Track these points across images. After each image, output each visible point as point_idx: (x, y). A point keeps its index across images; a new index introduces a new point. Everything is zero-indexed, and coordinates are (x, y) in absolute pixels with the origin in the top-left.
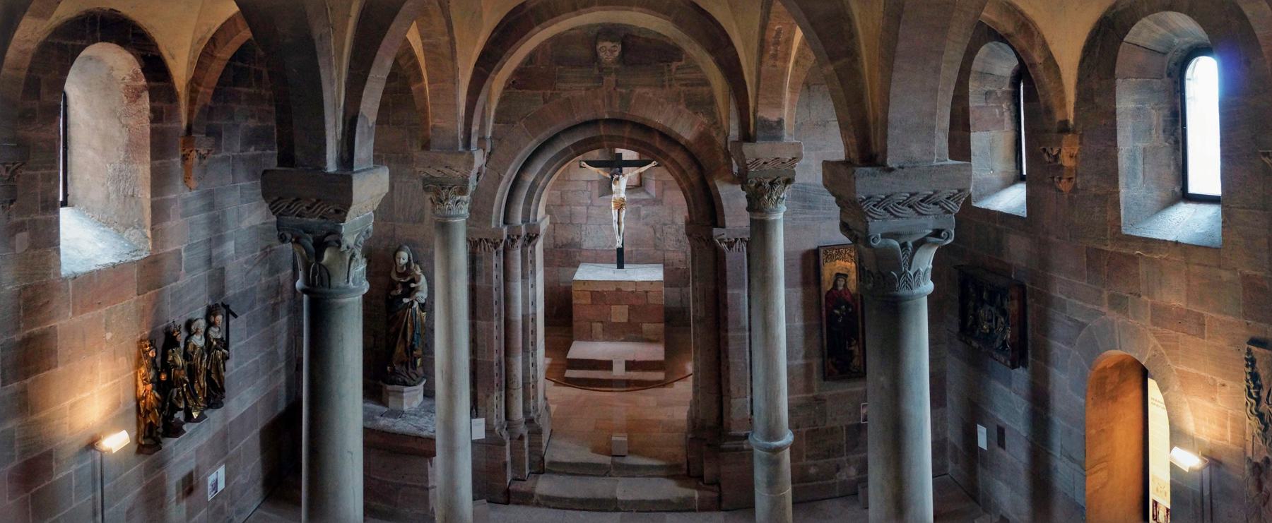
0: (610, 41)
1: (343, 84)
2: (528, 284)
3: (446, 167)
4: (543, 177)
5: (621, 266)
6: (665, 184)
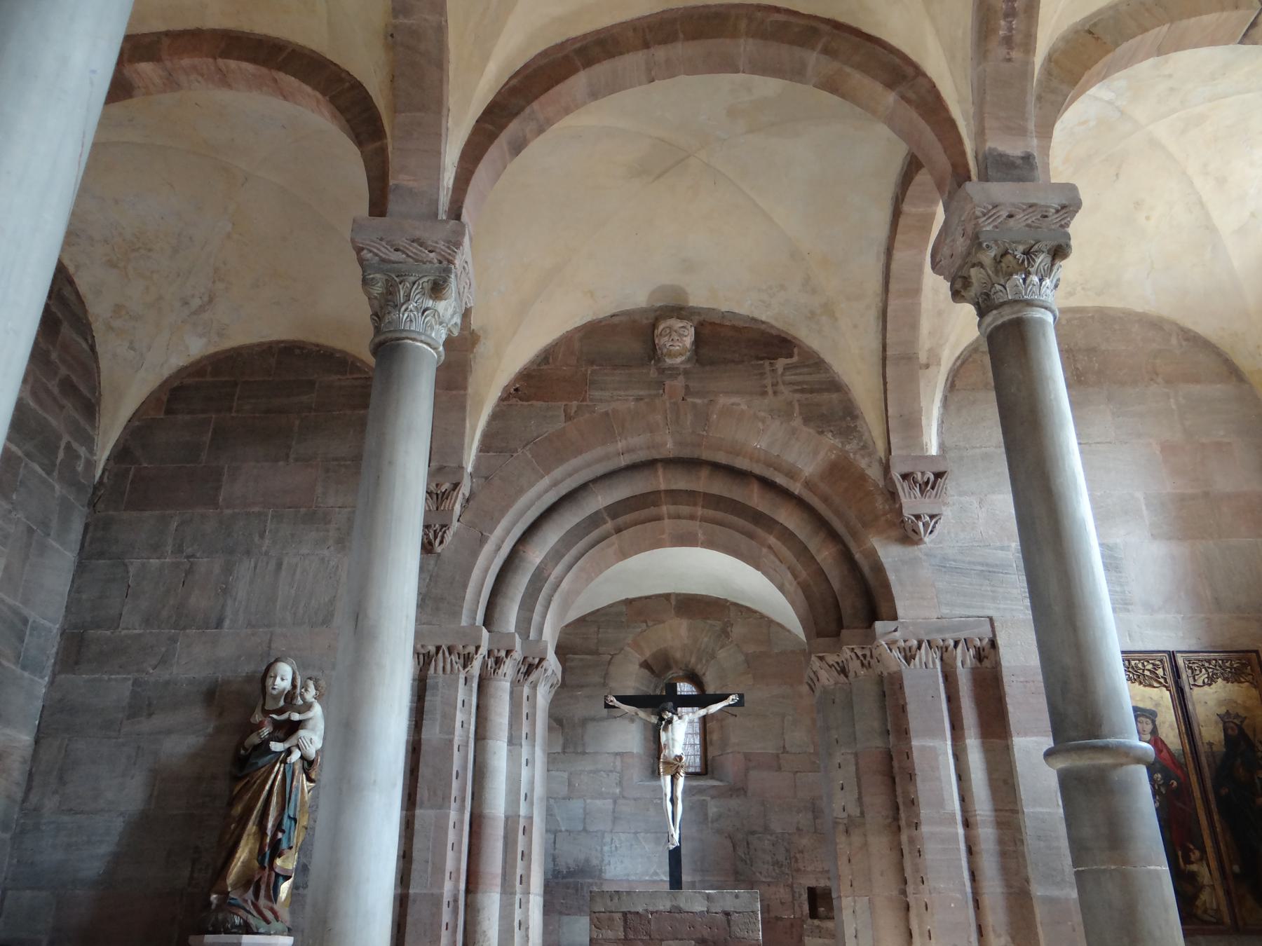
0: (678, 318)
2: (520, 756)
3: (413, 241)
4: (556, 565)
6: (750, 760)
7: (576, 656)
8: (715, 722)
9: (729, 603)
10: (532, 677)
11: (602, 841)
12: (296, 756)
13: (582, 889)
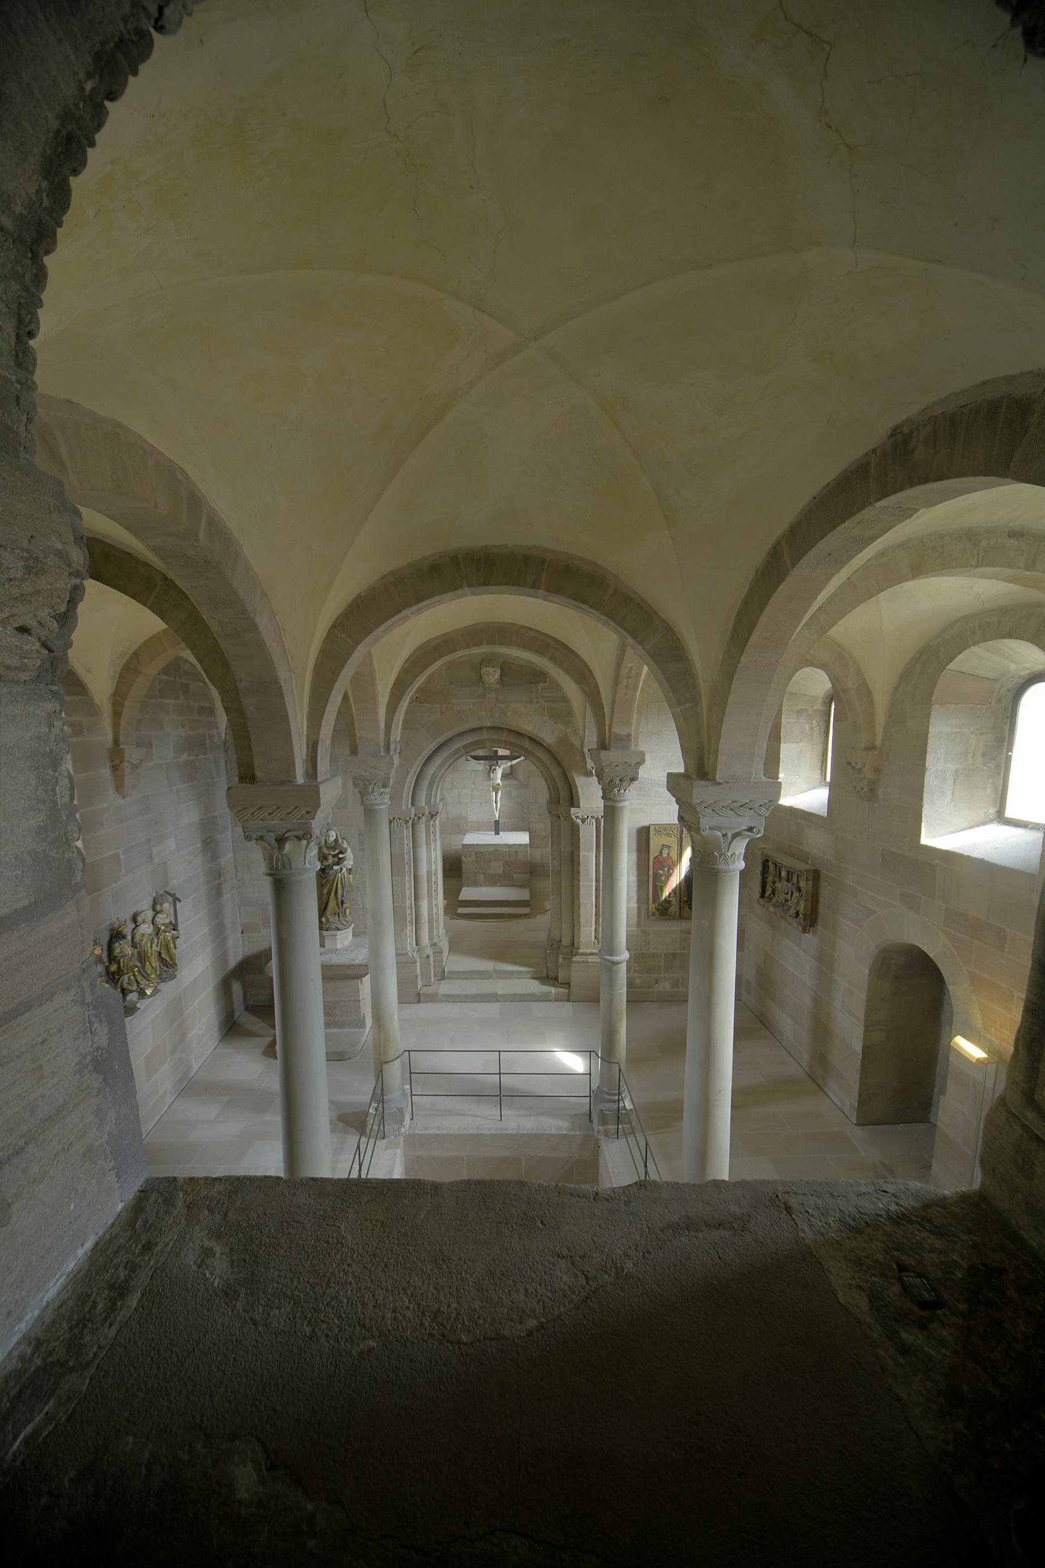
1: (305, 716)
5: (497, 833)
10: (434, 819)
12: (344, 869)
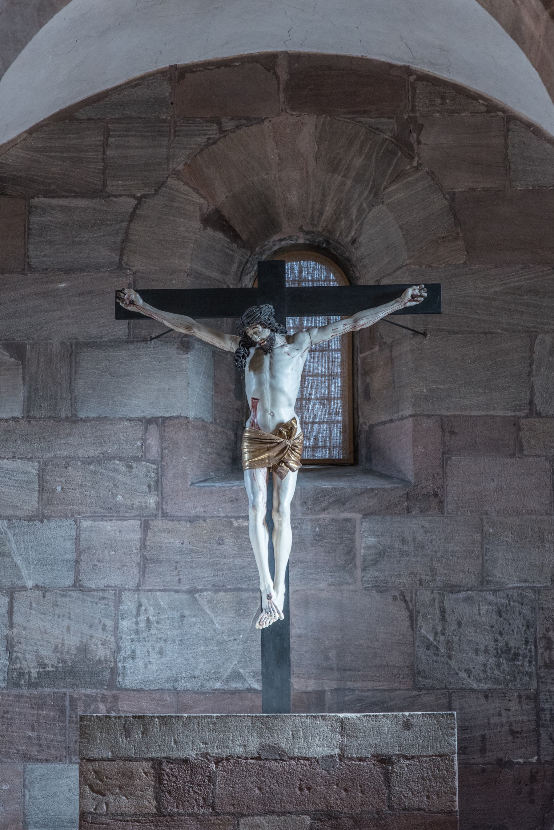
6: (452, 433)
7: (55, 202)
8: (377, 348)
9: (412, 78)
11: (117, 608)
13: (73, 707)
